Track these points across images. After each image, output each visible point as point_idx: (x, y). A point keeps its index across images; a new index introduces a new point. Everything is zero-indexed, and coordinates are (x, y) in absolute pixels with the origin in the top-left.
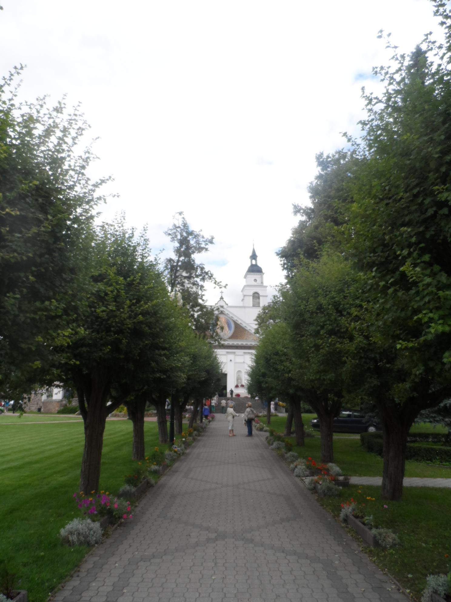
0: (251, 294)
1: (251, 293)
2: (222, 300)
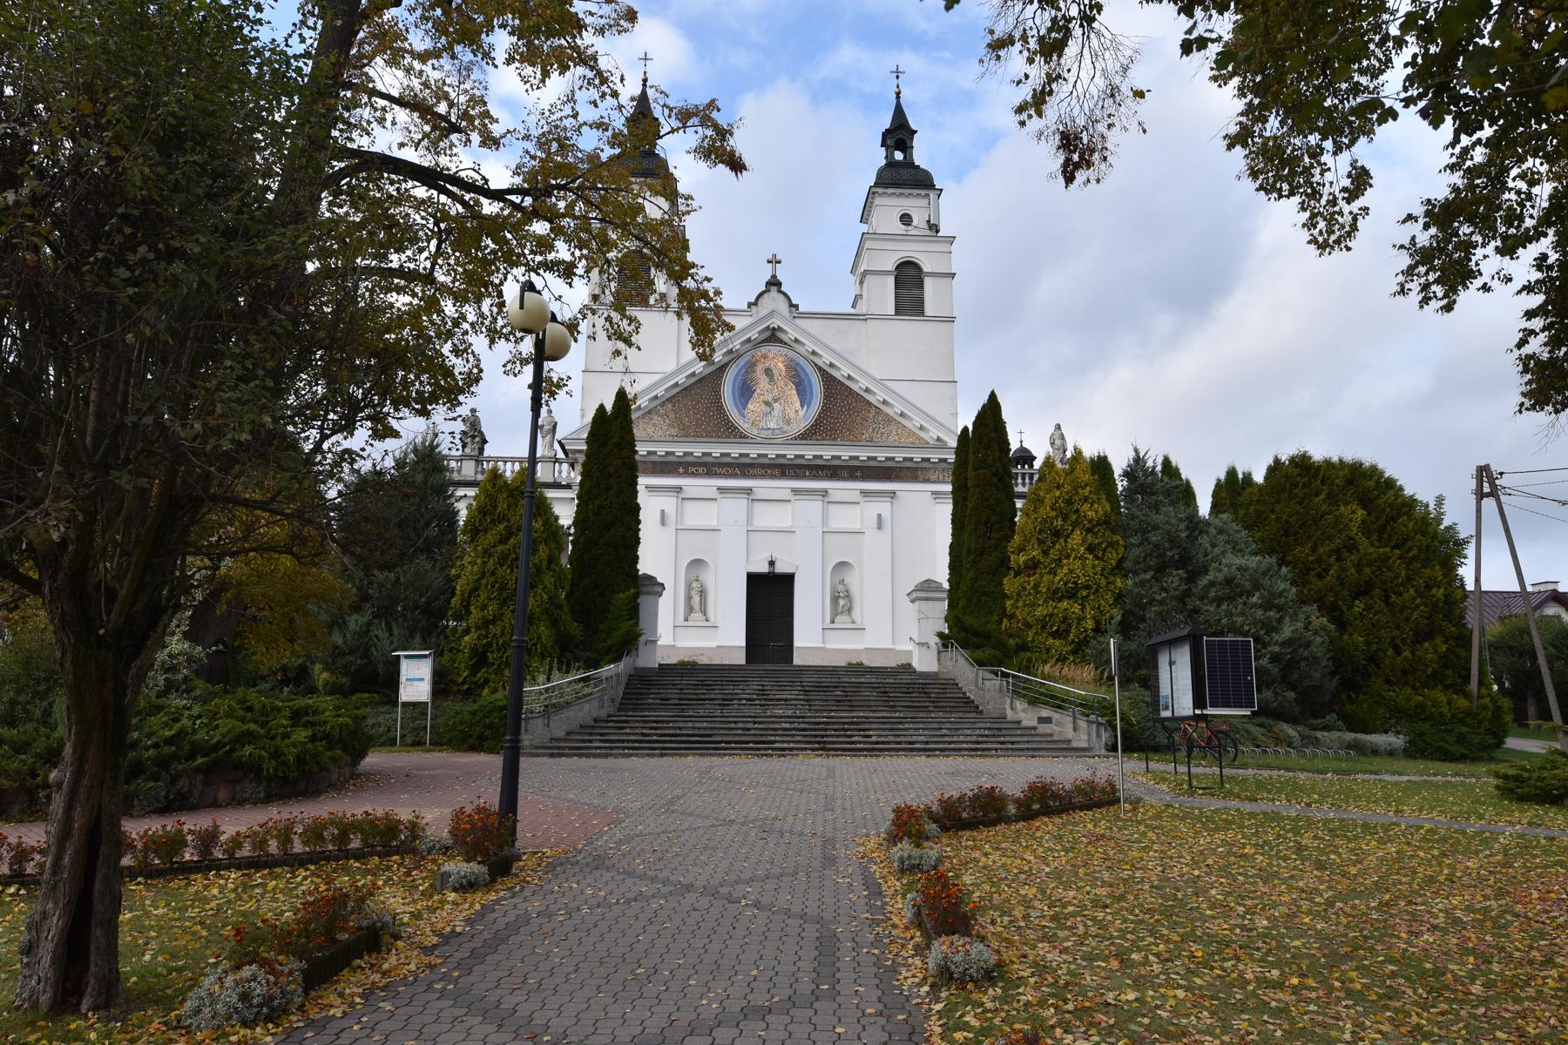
0: (891, 266)
2: (774, 289)
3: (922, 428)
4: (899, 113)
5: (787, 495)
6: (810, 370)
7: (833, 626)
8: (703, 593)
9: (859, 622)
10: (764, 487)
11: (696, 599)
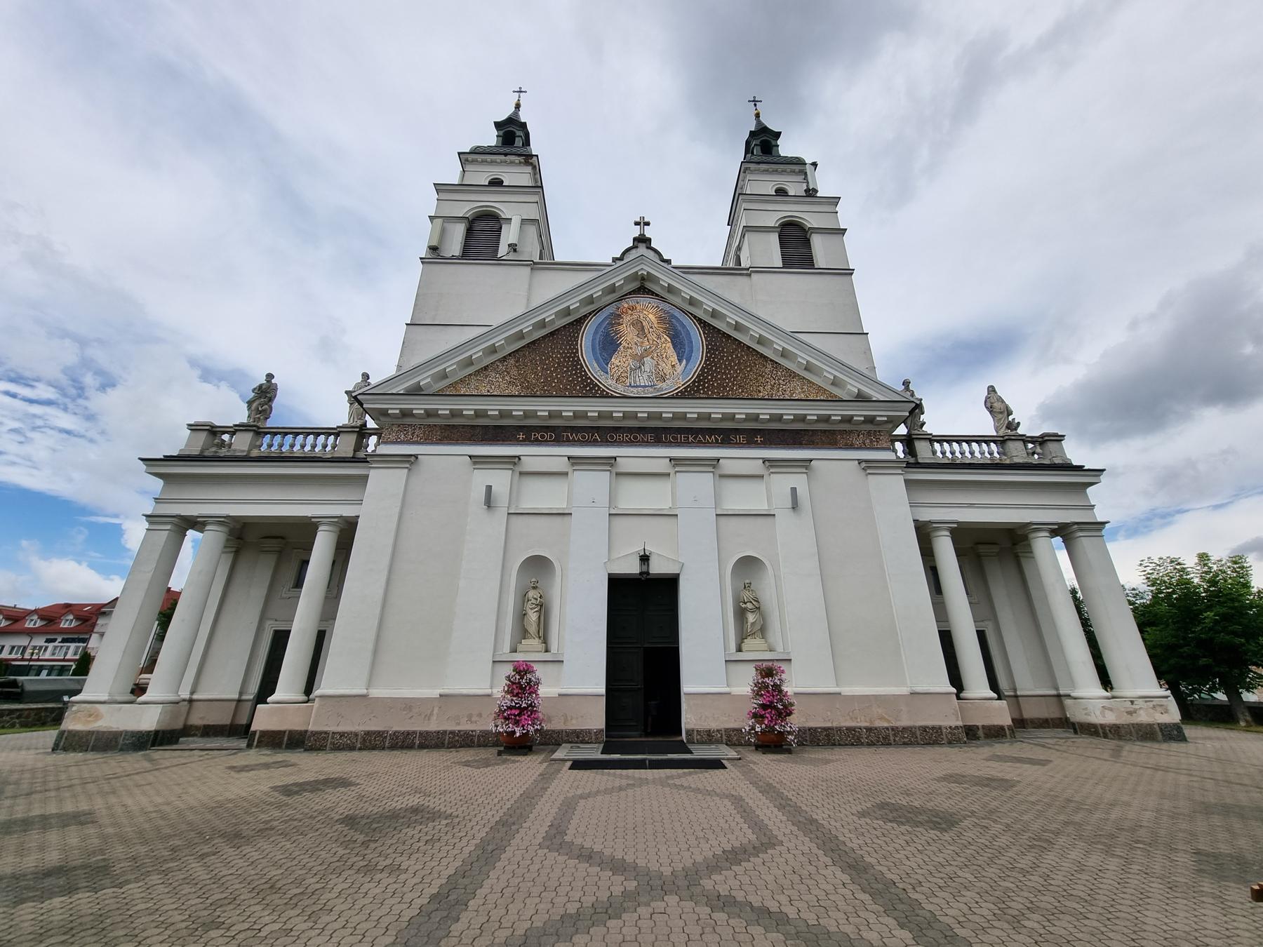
1: (772, 220)
3: (835, 383)
4: (759, 122)
8: (543, 609)
9: (780, 649)
10: (632, 456)
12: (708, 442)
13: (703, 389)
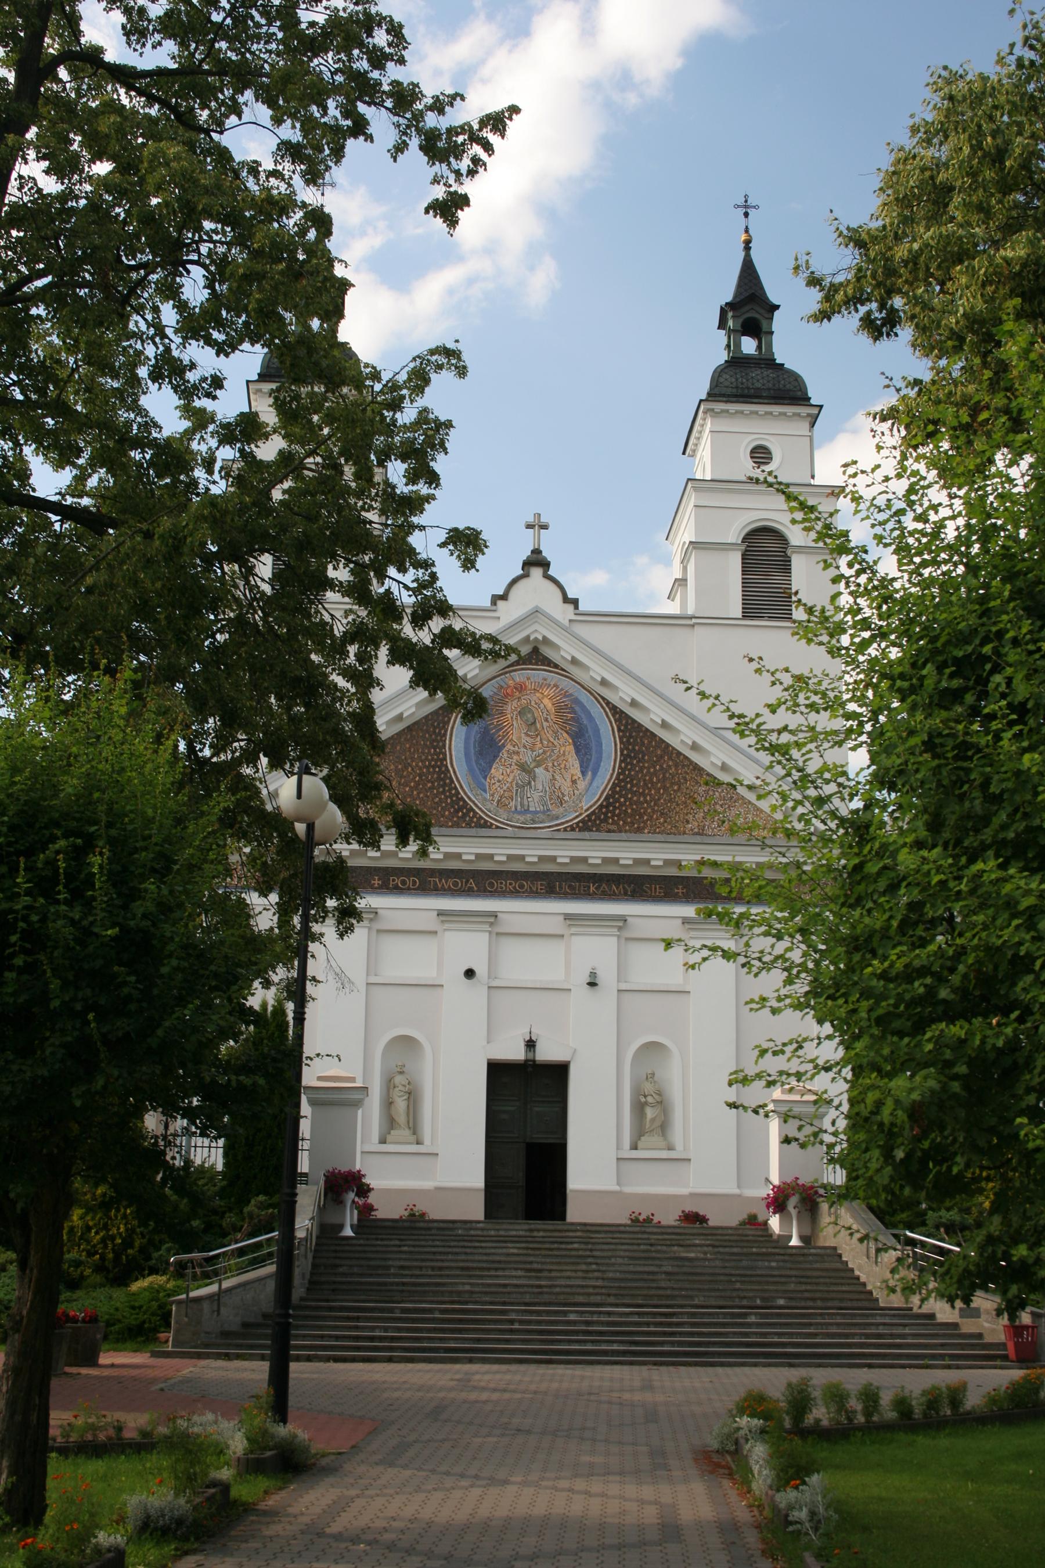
0: (734, 534)
2: (536, 572)
4: (749, 274)
5: (556, 925)
6: (597, 712)
7: (635, 1154)
8: (413, 1096)
11: (401, 1104)
12: (615, 894)
13: (612, 817)
